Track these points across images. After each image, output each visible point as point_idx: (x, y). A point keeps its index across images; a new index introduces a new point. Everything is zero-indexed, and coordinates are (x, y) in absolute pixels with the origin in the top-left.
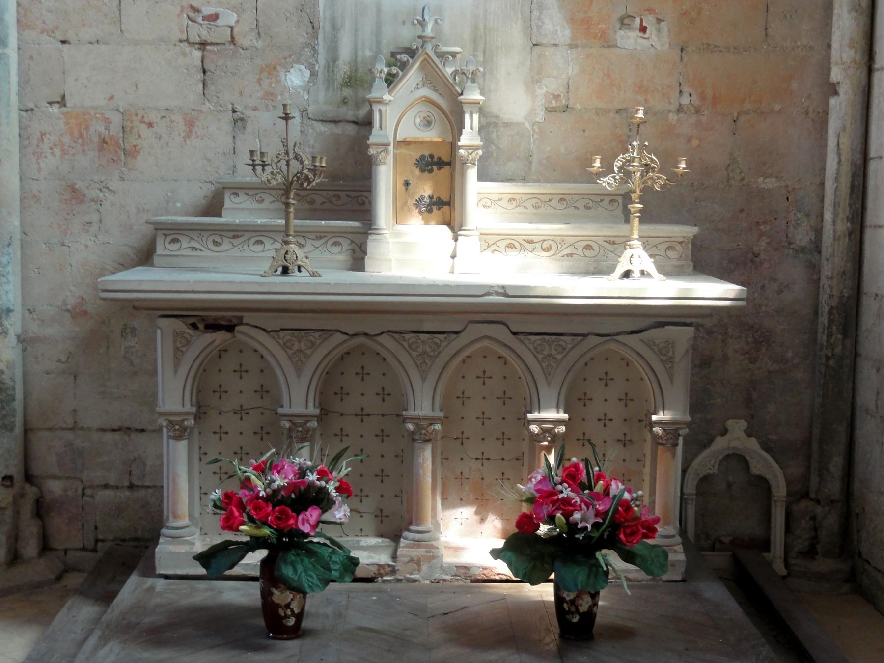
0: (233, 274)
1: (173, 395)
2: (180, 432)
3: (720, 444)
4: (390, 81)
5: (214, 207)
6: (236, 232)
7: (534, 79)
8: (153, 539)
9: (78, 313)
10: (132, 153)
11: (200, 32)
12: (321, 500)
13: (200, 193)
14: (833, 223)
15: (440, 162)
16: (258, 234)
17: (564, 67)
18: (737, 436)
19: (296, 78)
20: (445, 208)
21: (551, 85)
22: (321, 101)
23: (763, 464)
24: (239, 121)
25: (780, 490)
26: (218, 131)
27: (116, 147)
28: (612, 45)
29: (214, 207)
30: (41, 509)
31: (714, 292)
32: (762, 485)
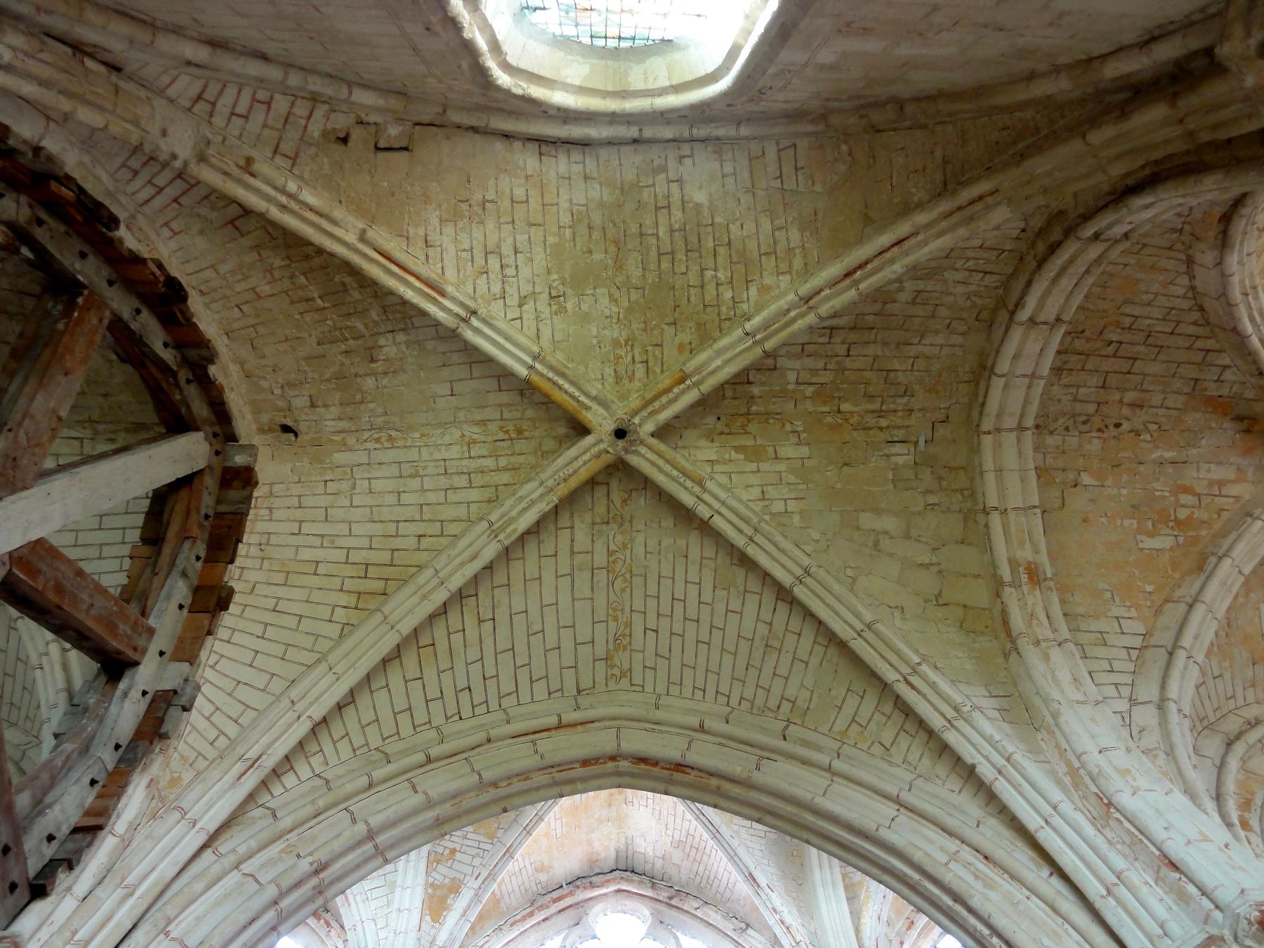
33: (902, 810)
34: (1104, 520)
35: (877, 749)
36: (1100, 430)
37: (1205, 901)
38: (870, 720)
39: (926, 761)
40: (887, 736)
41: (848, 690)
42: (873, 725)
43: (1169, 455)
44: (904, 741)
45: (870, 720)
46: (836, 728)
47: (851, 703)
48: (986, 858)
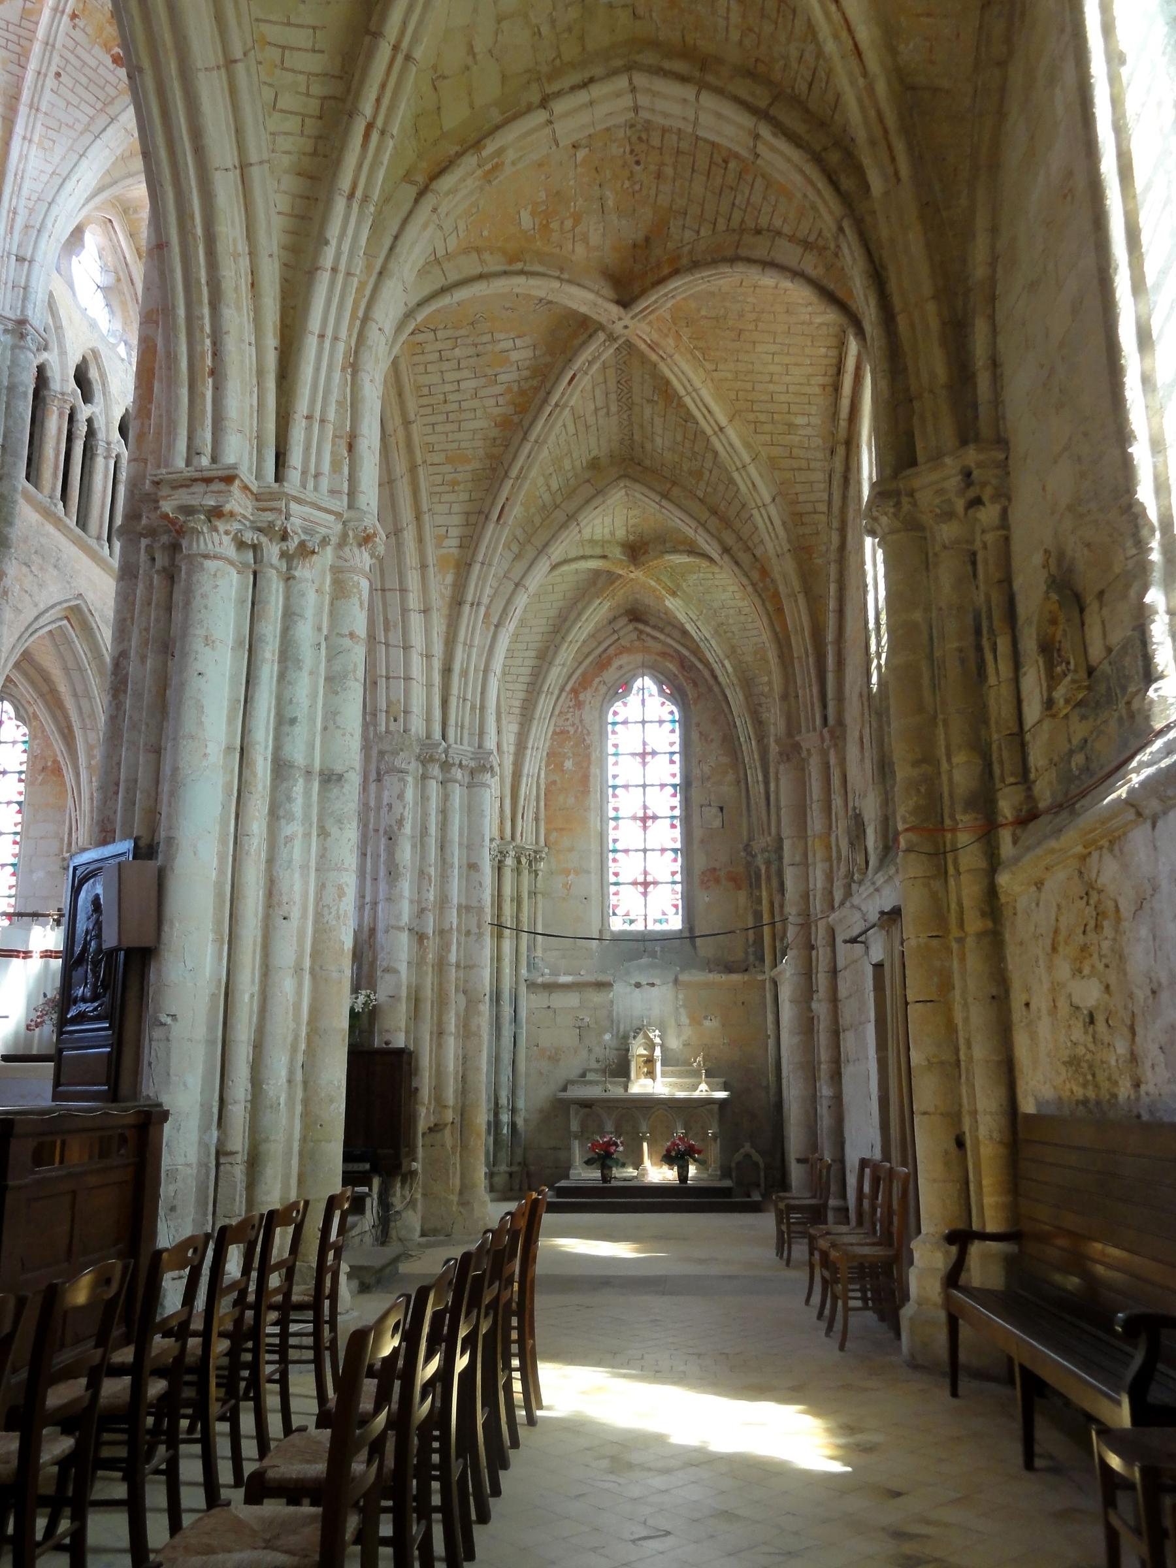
0: (593, 1092)
1: (575, 1126)
2: (576, 1138)
3: (742, 1151)
4: (635, 1037)
5: (583, 1075)
6: (591, 1083)
7: (679, 1036)
8: (569, 1168)
9: (541, 1111)
10: (558, 1060)
11: (579, 1023)
12: (616, 1144)
13: (580, 1071)
14: (772, 1078)
15: (650, 1061)
16: (596, 1083)
17: (688, 1032)
18: (747, 1148)
19: (607, 1037)
20: (651, 1074)
21: (684, 1037)
22: (614, 1044)
23: (756, 1157)
24: (590, 1050)
25: (762, 1165)
26: (584, 1053)
27: (554, 1059)
28: (701, 1024)
29: (583, 1075)
30: (528, 1175)
31: (722, 1095)
32: (756, 1164)
33: (238, 171)
34: (543, 177)
35: (268, 94)
36: (632, 151)
37: (346, 484)
38: (293, 71)
39: (286, 160)
40: (286, 101)
41: (314, 28)
42: (289, 77)
43: (610, 203)
44: (292, 124)
45: (293, 71)
46: (265, 28)
47: (300, 38)
48: (253, 285)
